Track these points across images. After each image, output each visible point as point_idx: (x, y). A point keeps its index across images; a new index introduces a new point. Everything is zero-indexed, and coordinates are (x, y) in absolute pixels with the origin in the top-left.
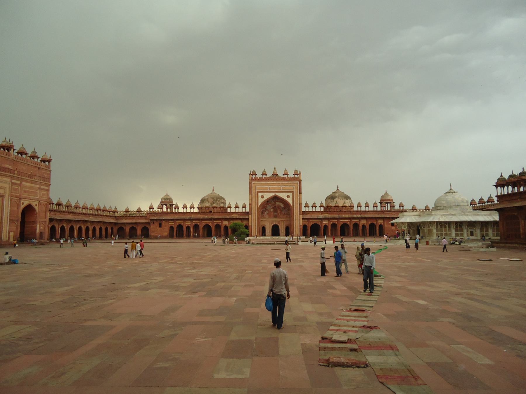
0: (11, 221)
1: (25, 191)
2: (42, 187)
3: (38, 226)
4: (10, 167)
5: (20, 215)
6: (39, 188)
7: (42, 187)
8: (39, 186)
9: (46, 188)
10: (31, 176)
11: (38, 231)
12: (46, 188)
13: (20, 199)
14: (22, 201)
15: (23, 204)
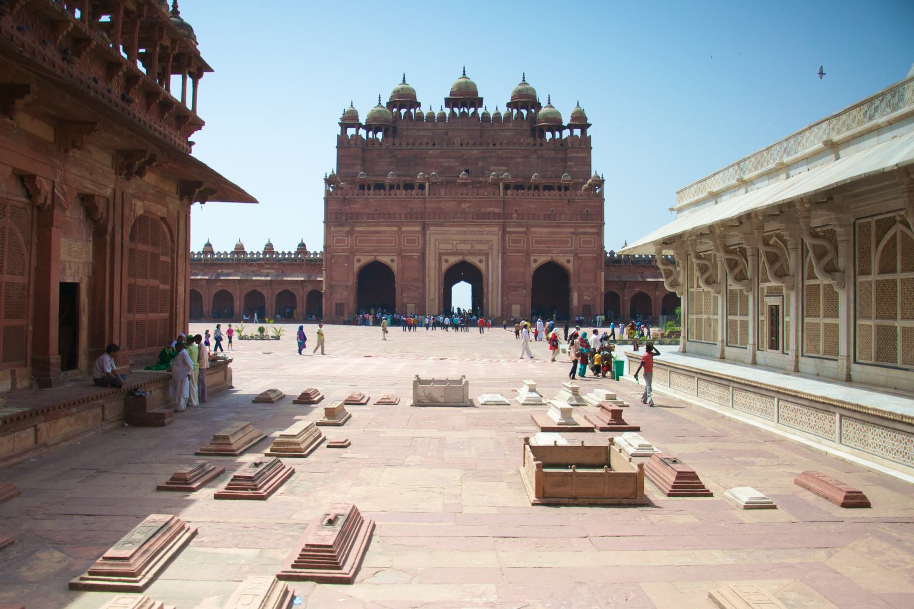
0: (507, 289)
1: (537, 242)
2: (580, 230)
3: (575, 296)
4: (497, 210)
5: (529, 279)
6: (573, 233)
7: (580, 230)
8: (572, 230)
9: (594, 230)
10: (548, 217)
11: (575, 302)
12: (594, 230)
13: (528, 254)
14: (532, 258)
15: (535, 261)
